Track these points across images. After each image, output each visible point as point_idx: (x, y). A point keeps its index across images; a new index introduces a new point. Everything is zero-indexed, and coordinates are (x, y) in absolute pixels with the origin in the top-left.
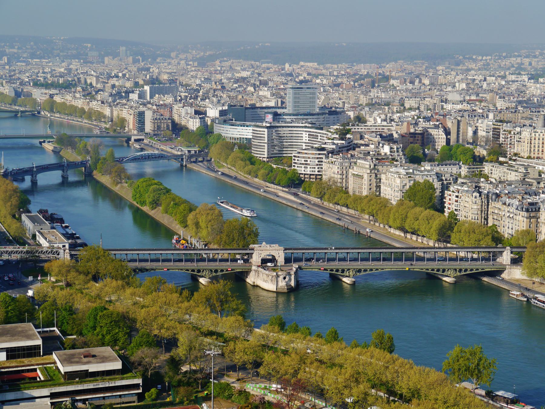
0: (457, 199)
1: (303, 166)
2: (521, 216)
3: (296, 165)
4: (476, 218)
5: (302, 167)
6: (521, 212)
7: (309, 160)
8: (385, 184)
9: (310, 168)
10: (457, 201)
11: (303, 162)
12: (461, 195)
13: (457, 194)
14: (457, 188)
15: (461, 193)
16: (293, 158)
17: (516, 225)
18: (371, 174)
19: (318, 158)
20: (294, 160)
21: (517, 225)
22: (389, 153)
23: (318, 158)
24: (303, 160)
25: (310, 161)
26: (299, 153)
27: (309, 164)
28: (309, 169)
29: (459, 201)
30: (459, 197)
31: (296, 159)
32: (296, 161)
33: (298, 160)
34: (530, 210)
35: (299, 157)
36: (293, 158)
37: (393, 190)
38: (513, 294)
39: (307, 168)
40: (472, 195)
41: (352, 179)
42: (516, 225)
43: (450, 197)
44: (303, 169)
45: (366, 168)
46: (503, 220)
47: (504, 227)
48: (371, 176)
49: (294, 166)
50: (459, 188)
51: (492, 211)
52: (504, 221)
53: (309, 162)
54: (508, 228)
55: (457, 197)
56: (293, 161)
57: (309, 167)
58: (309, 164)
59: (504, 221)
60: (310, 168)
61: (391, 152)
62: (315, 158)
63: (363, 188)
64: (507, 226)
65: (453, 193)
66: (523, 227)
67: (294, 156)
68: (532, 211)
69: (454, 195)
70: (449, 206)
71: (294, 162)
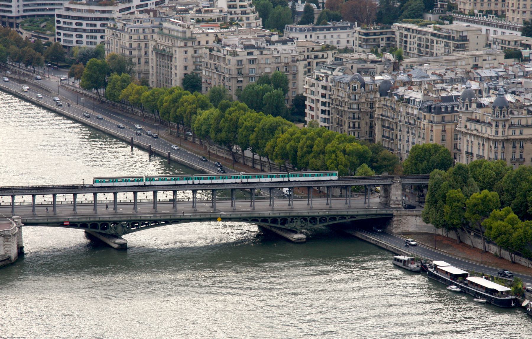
0: (324, 91)
1: (74, 34)
2: (427, 121)
3: (62, 32)
4: (357, 125)
5: (72, 36)
6: (427, 115)
7: (84, 23)
8: (209, 66)
9: (87, 37)
10: (324, 96)
11: (74, 26)
12: (331, 85)
13: (324, 83)
14: (325, 73)
15: (332, 82)
16: (56, 19)
17: (419, 137)
18: (185, 49)
19: (101, 19)
20: (58, 22)
21: (422, 136)
22: (226, 9)
23: (101, 19)
24: (74, 22)
25: (87, 25)
26: (68, 9)
27: (84, 31)
28: (84, 39)
29: (327, 96)
30: (329, 88)
31: (62, 20)
32: (61, 25)
33: (65, 23)
34: (443, 110)
35: (65, 17)
36: (56, 19)
37: (222, 78)
38: (400, 261)
39: (81, 36)
40: (349, 86)
41: (154, 57)
42: (419, 137)
43: (313, 89)
44: (74, 39)
45: (177, 38)
46: (399, 128)
47: (400, 140)
48: (186, 52)
49: (59, 34)
50: (329, 72)
51: (381, 113)
52: (400, 131)
53: (84, 27)
54: (408, 141)
55: (324, 87)
56: (57, 24)
57: (84, 35)
58: (84, 31)
59: (400, 131)
60: (87, 37)
61: (230, 7)
62: (96, 19)
63: (173, 73)
64: (406, 139)
65: (319, 82)
66: (432, 140)
67: (59, 16)
68: (446, 112)
69: (320, 86)
70: (313, 105)
71: (58, 27)
